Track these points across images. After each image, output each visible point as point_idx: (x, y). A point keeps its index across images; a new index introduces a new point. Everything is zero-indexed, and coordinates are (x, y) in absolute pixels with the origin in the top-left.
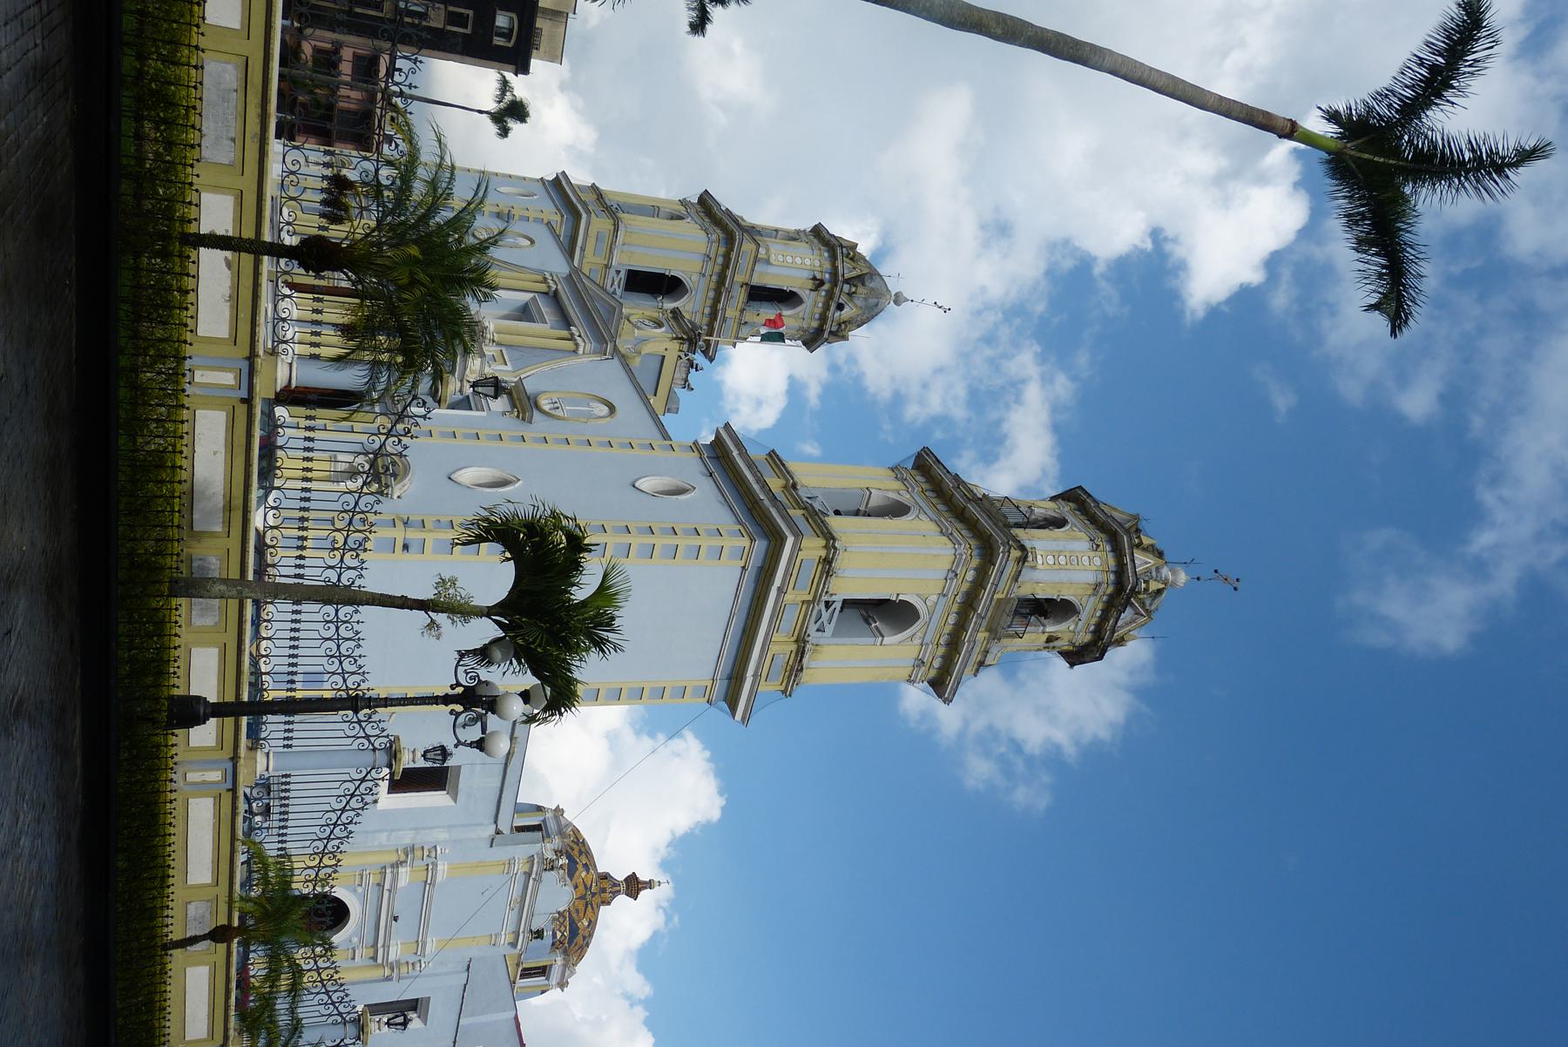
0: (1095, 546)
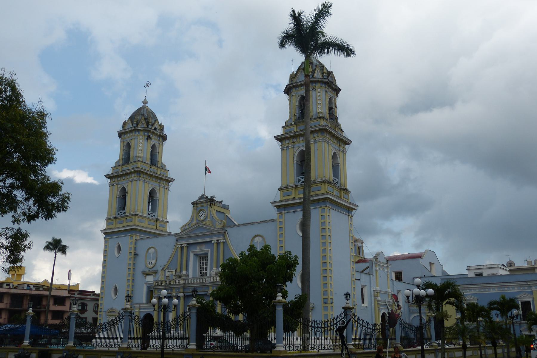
0: (314, 90)
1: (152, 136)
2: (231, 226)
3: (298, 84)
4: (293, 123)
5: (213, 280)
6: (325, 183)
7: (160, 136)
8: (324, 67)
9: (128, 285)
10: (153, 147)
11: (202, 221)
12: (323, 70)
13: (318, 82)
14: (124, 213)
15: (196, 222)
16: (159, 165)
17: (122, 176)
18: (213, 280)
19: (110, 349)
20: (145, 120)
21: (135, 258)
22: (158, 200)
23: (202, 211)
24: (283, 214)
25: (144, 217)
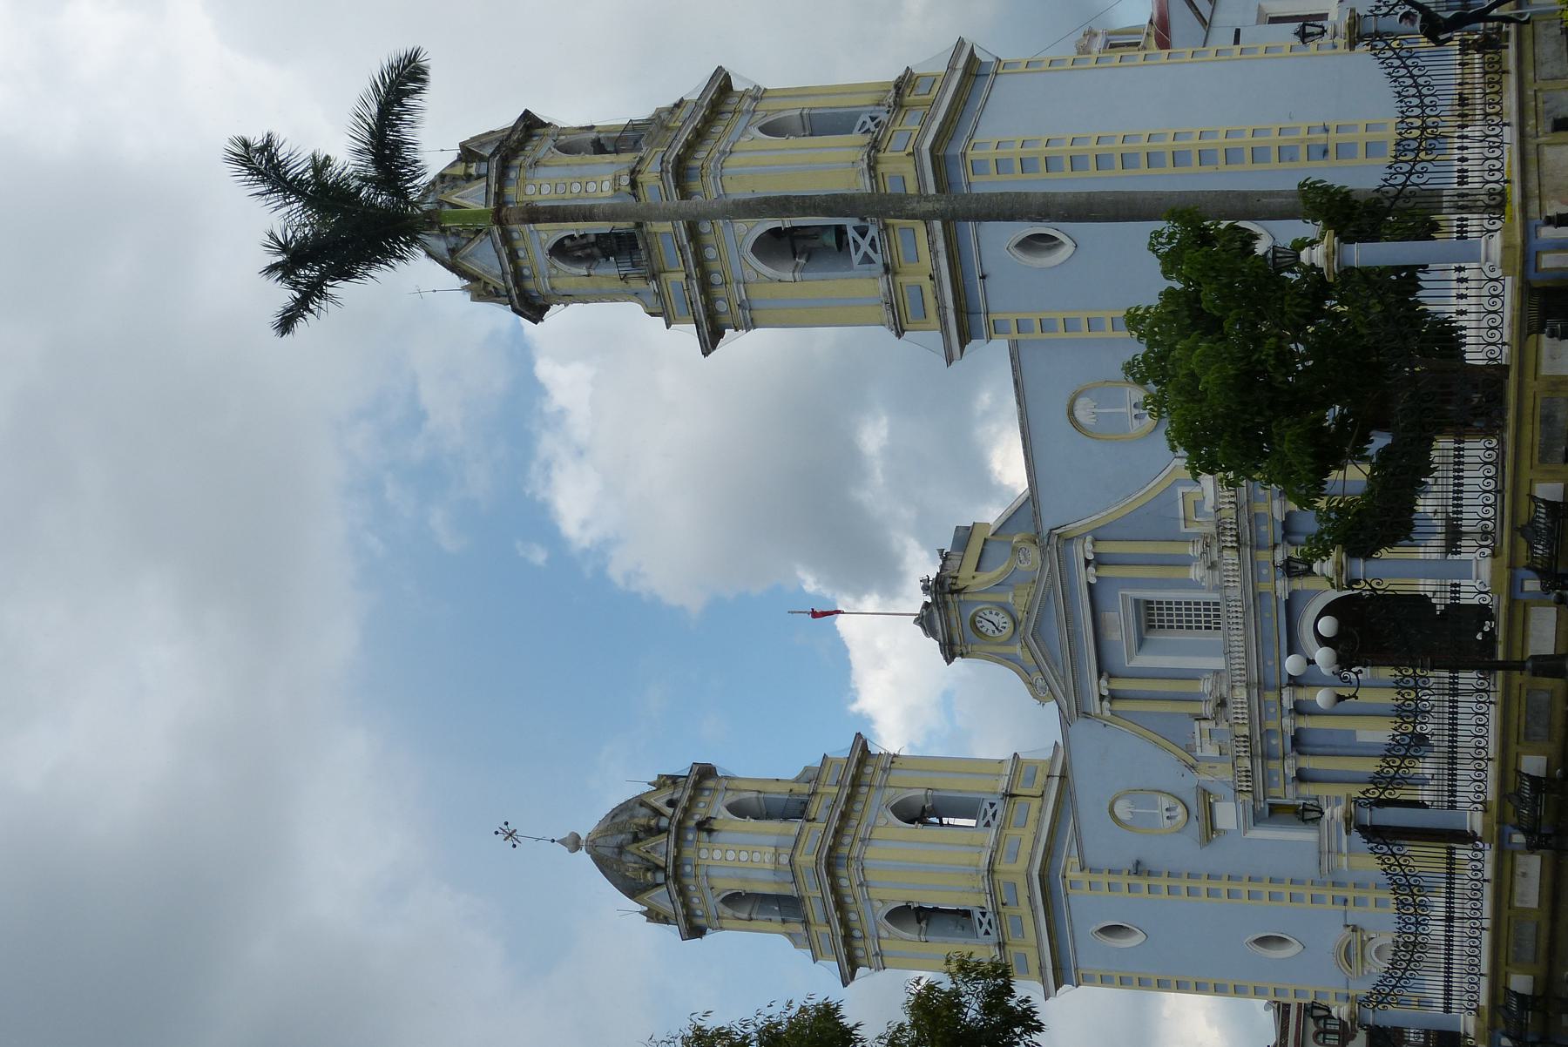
1: (697, 817)
2: (1036, 515)
3: (509, 268)
4: (653, 285)
5: (1233, 576)
6: (877, 162)
7: (698, 788)
8: (447, 172)
9: (1250, 895)
10: (738, 810)
11: (1016, 623)
12: (454, 178)
13: (500, 195)
14: (984, 914)
15: (1018, 646)
16: (806, 789)
17: (845, 923)
18: (1237, 579)
19: (1486, 923)
20: (641, 840)
21: (1150, 873)
22: (936, 793)
23: (979, 625)
24: (992, 317)
25: (998, 842)
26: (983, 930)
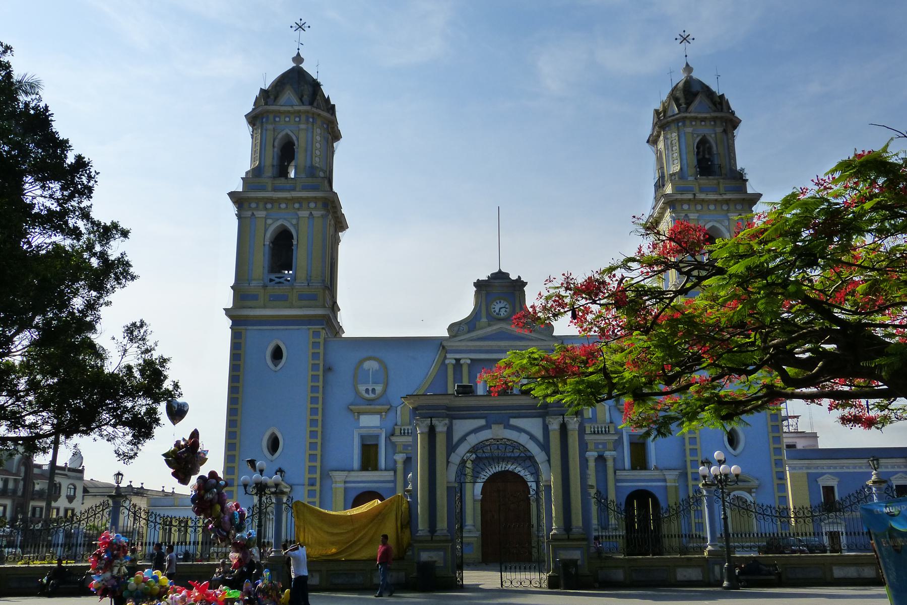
26: (274, 278)
